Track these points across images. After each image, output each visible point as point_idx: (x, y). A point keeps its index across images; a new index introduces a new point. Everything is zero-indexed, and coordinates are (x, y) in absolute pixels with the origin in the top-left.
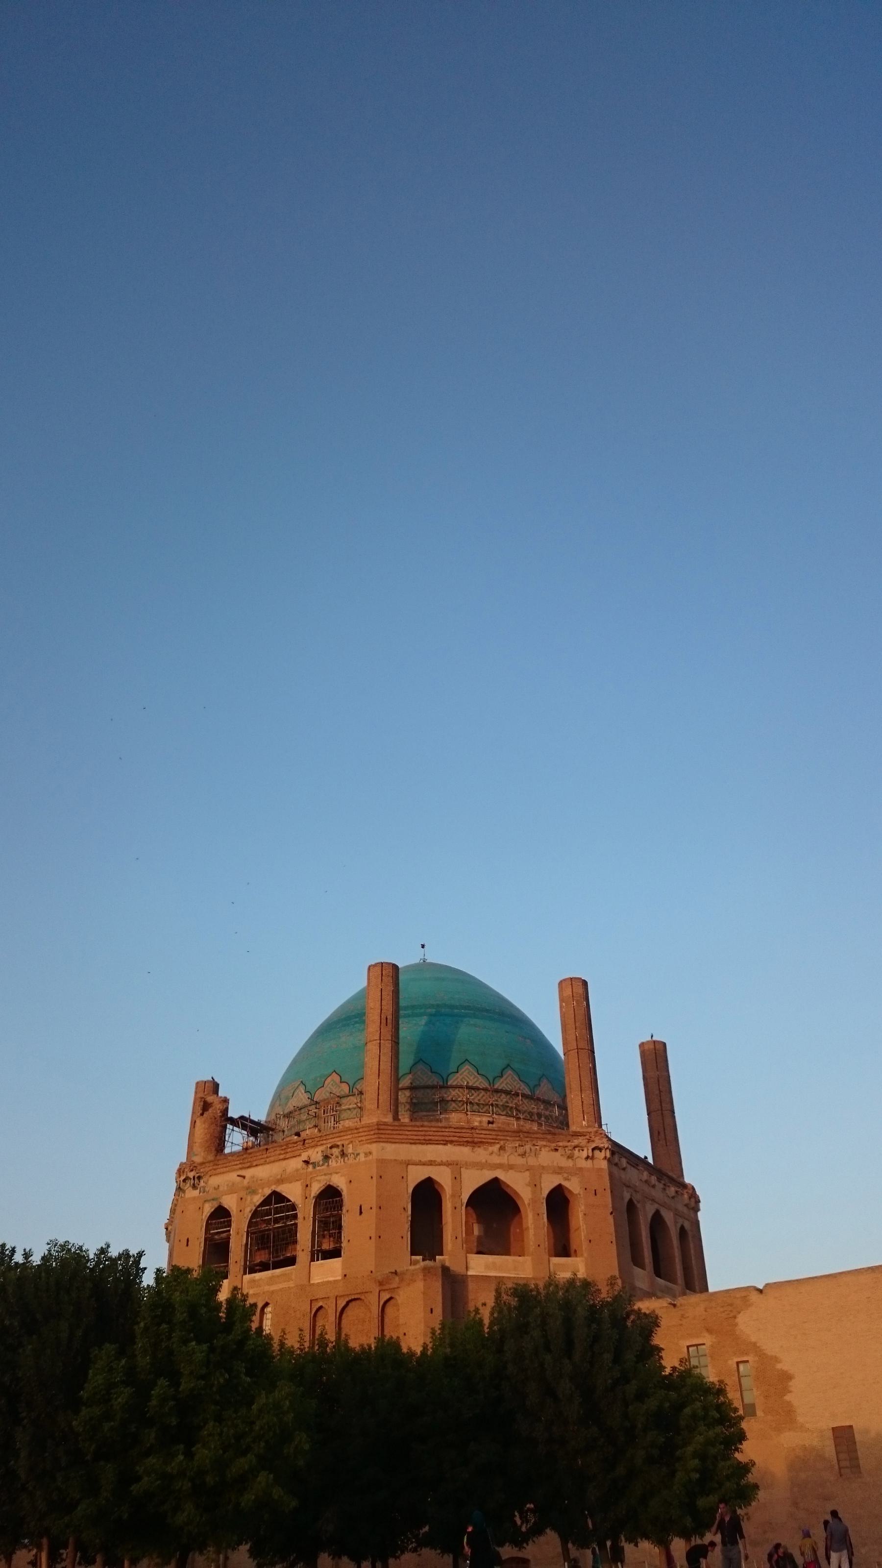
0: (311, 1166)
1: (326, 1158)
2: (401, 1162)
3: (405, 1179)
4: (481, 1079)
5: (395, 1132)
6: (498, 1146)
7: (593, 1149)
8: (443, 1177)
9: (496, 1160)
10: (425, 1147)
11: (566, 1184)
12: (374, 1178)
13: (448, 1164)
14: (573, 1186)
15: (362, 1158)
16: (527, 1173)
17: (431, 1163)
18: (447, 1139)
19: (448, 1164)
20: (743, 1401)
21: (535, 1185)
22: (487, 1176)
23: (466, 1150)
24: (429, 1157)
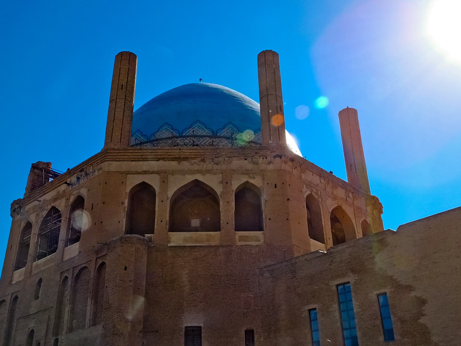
0: (70, 186)
1: (78, 178)
2: (122, 173)
3: (124, 184)
4: (207, 131)
5: (120, 154)
6: (200, 159)
7: (275, 157)
8: (154, 181)
9: (196, 167)
10: (141, 163)
11: (252, 181)
12: (101, 184)
13: (158, 173)
14: (256, 182)
15: (96, 173)
16: (221, 175)
17: (145, 172)
18: (159, 157)
19: (158, 173)
20: (383, 328)
21: (226, 183)
22: (190, 178)
23: (174, 163)
24: (145, 169)
